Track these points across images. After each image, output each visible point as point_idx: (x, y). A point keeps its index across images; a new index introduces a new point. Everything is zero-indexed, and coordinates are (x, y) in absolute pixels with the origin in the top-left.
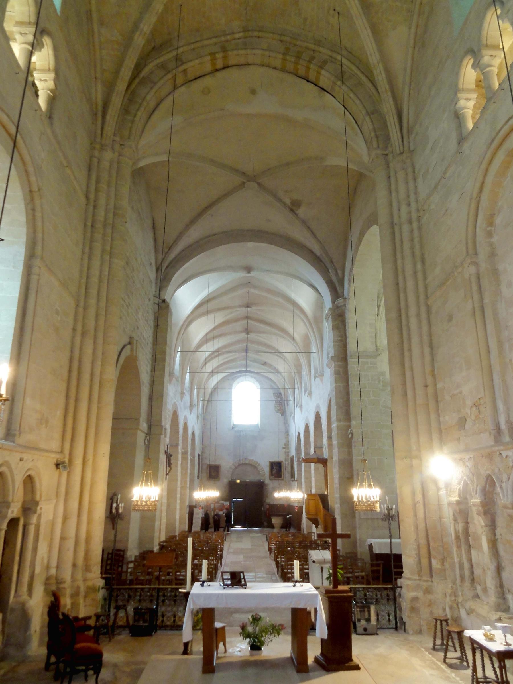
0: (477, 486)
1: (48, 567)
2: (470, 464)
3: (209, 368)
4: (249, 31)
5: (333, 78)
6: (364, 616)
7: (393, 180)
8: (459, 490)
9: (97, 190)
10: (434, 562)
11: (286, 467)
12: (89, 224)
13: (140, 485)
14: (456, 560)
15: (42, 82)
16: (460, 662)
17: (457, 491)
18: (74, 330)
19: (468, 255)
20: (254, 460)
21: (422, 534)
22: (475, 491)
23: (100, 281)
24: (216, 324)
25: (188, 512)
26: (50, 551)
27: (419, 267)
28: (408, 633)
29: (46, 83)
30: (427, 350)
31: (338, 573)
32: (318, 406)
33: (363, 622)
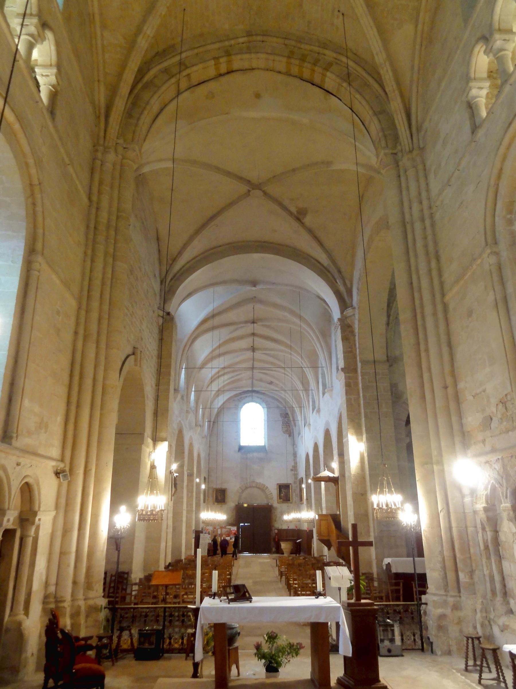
0: (507, 489)
1: (47, 584)
2: (498, 466)
3: (215, 387)
4: (252, 35)
5: (338, 80)
6: (388, 636)
7: (403, 179)
8: (487, 496)
9: (100, 192)
10: (461, 575)
11: (294, 487)
12: (92, 226)
13: (145, 493)
14: (486, 572)
15: (44, 78)
16: (497, 684)
17: (484, 497)
18: (76, 333)
19: (487, 245)
21: (446, 546)
22: (505, 495)
23: (103, 284)
24: (222, 341)
25: (194, 536)
26: (48, 568)
27: (434, 264)
28: (436, 655)
29: (48, 78)
30: (445, 349)
31: (361, 585)
32: (327, 423)
33: (387, 643)
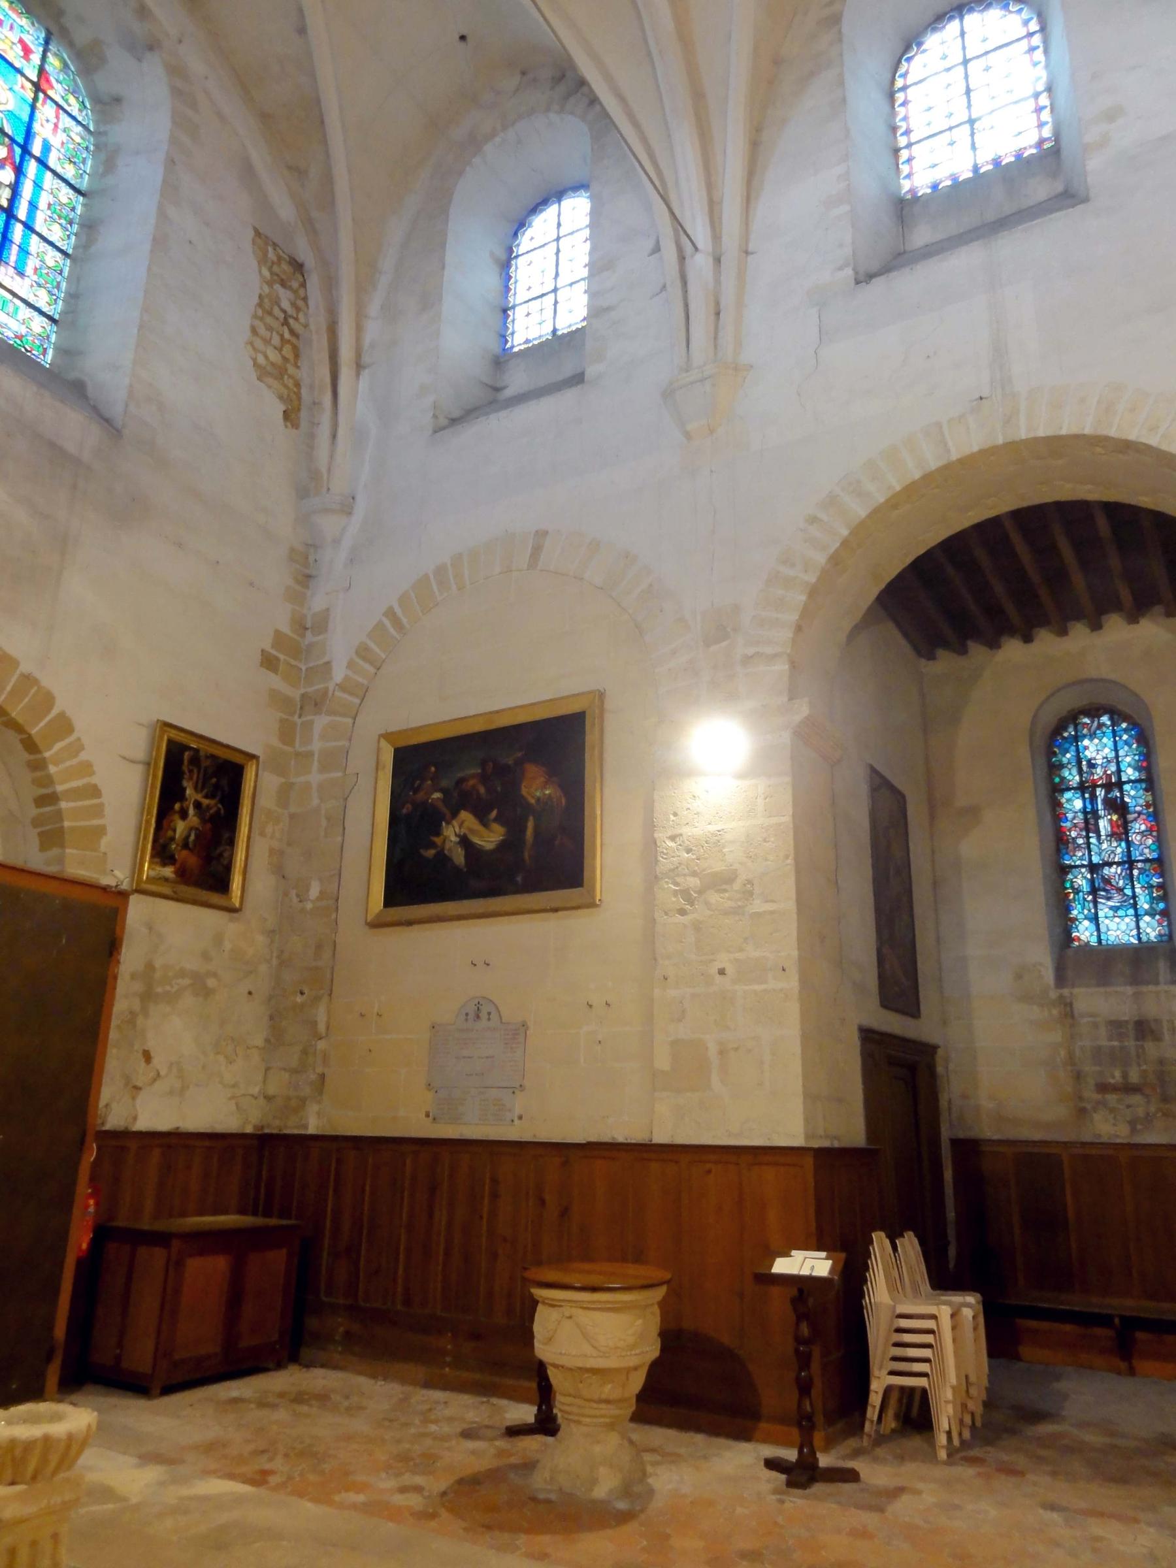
20: (25, 667)
